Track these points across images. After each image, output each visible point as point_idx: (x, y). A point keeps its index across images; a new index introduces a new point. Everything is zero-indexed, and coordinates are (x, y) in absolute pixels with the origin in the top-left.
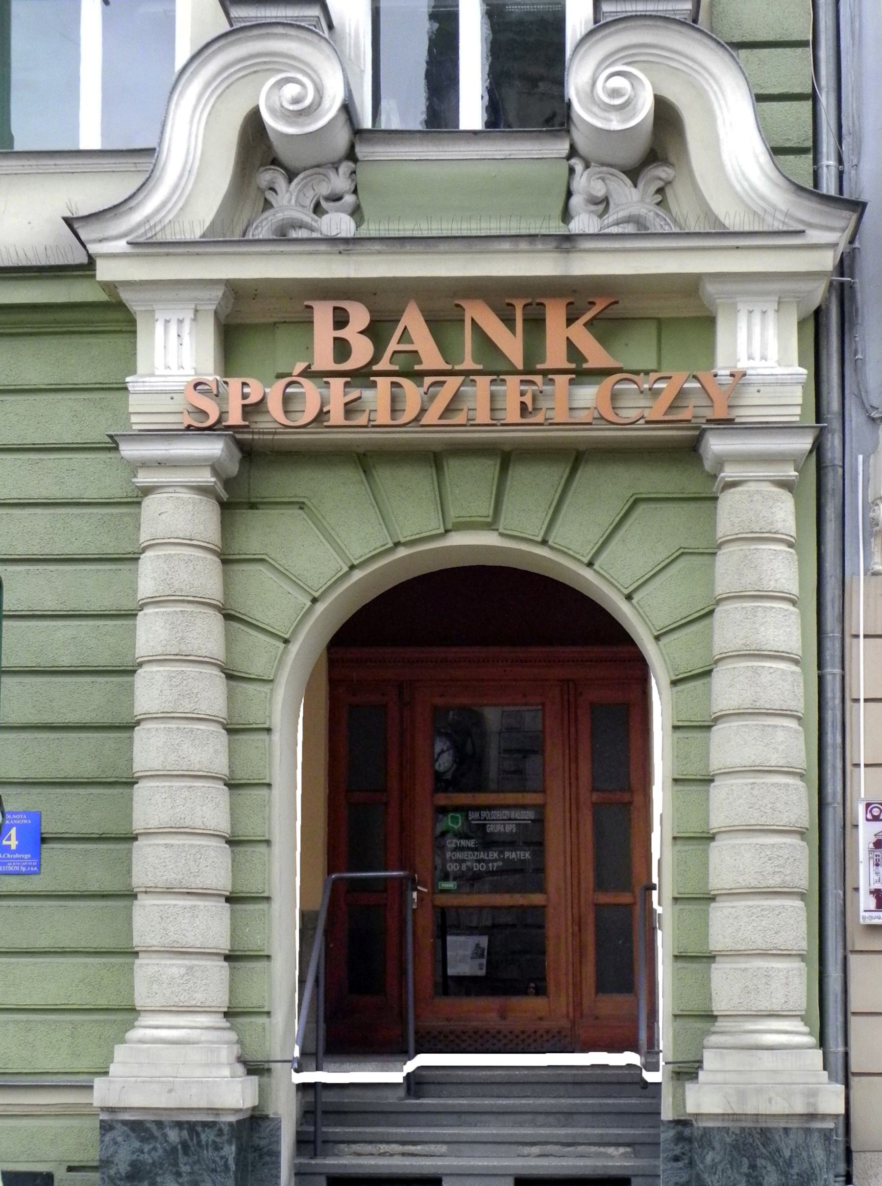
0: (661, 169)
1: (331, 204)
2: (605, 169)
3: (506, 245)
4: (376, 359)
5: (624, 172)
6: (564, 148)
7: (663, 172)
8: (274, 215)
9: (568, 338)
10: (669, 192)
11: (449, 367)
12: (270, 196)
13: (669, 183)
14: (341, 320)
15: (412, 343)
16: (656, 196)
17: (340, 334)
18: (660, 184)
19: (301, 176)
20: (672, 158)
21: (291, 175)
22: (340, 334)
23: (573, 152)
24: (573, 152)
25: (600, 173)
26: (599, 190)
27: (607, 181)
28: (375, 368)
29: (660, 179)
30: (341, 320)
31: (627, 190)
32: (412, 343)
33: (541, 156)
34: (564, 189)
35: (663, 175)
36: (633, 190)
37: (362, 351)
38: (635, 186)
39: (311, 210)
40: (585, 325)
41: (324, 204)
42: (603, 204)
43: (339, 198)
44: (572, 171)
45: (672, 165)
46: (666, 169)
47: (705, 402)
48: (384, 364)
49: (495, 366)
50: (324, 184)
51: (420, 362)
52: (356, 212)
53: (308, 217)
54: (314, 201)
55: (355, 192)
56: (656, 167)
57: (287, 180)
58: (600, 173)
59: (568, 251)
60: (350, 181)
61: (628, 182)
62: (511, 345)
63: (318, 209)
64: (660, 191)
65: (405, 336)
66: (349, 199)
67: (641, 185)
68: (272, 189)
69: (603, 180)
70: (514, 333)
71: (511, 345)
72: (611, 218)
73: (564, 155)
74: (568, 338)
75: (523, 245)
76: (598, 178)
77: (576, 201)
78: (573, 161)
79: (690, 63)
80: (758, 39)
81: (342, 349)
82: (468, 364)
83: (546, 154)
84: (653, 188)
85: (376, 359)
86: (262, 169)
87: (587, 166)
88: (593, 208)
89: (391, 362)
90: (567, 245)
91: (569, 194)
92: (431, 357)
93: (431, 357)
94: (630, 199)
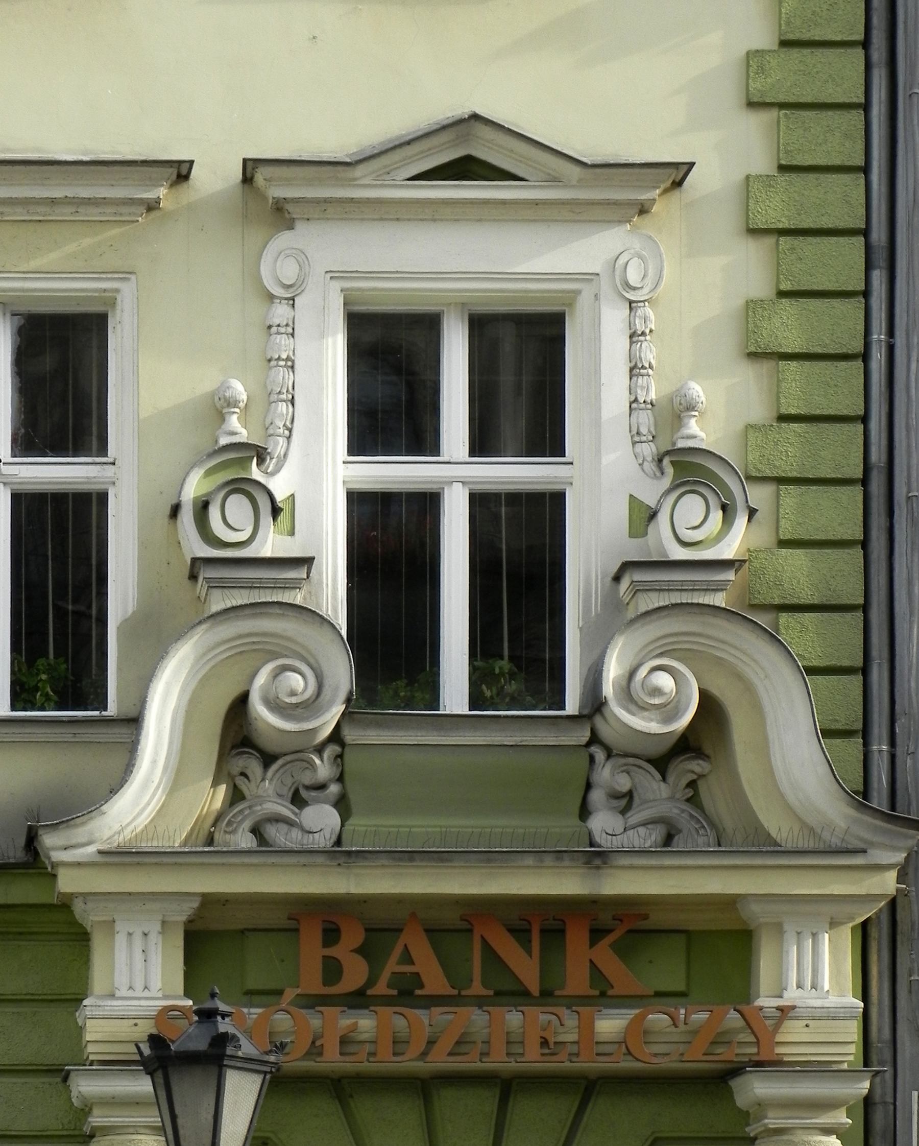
0: (696, 762)
1: (313, 794)
2: (631, 760)
3: (530, 861)
4: (371, 981)
5: (649, 761)
6: (584, 736)
7: (697, 766)
8: (250, 807)
9: (591, 961)
10: (702, 786)
11: (456, 992)
12: (241, 782)
13: (701, 776)
14: (331, 935)
15: (413, 963)
16: (687, 790)
17: (328, 952)
18: (695, 777)
19: (280, 762)
20: (708, 750)
21: (268, 759)
22: (328, 952)
23: (595, 739)
24: (595, 739)
25: (625, 765)
26: (623, 783)
27: (632, 774)
28: (369, 992)
29: (693, 772)
30: (331, 935)
31: (655, 785)
32: (413, 963)
33: (557, 744)
34: (584, 783)
35: (698, 769)
36: (662, 784)
37: (355, 973)
38: (664, 779)
39: (289, 800)
40: (610, 946)
41: (304, 793)
42: (625, 801)
43: (322, 787)
44: (592, 759)
45: (708, 757)
46: (701, 762)
47: (752, 1039)
48: (381, 988)
49: (514, 994)
50: (308, 773)
51: (421, 986)
52: (342, 805)
53: (286, 810)
54: (292, 790)
55: (340, 779)
56: (688, 759)
57: (262, 766)
58: (625, 765)
59: (598, 868)
60: (335, 768)
61: (658, 776)
62: (526, 968)
63: (298, 800)
64: (692, 784)
65: (407, 958)
66: (334, 789)
67: (671, 779)
68: (243, 774)
69: (628, 773)
70: (529, 953)
71: (526, 968)
72: (635, 817)
73: (584, 743)
74: (591, 961)
75: (549, 860)
76: (623, 772)
77: (597, 796)
78: (594, 749)
79: (733, 651)
80: (802, 602)
81: (332, 970)
82: (477, 988)
83: (563, 741)
84: (684, 782)
85: (371, 981)
86: (234, 752)
87: (609, 756)
88: (615, 803)
89: (389, 986)
90: (597, 862)
91: (588, 786)
92: (435, 980)
93: (435, 980)
94: (658, 794)
